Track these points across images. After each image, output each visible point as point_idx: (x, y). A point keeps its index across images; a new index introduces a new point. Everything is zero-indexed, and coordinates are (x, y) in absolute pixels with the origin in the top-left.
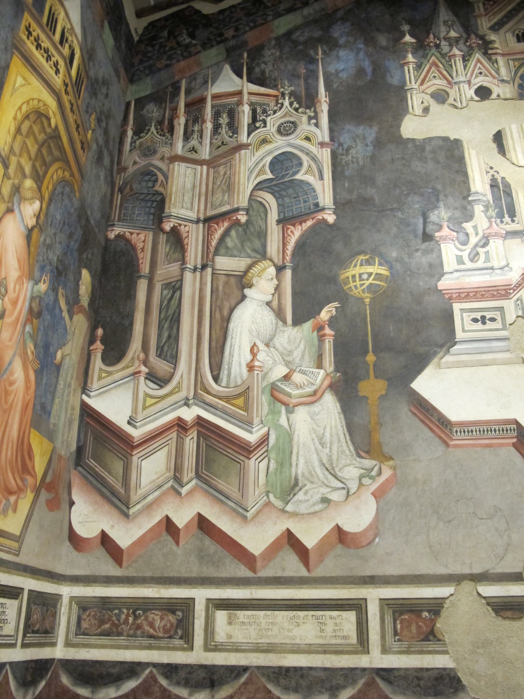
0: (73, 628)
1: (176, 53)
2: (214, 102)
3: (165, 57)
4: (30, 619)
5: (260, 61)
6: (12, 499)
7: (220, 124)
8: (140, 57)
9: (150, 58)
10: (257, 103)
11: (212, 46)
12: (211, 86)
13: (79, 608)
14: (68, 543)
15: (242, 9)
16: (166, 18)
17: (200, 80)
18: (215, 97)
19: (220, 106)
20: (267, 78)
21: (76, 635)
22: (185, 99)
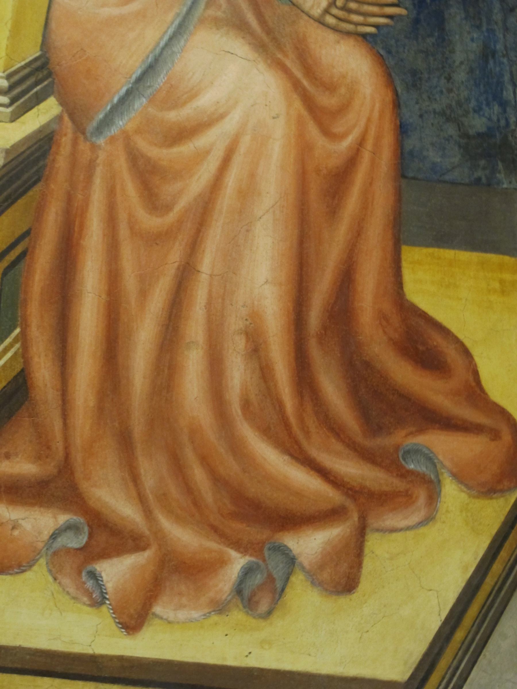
6: (309, 544)
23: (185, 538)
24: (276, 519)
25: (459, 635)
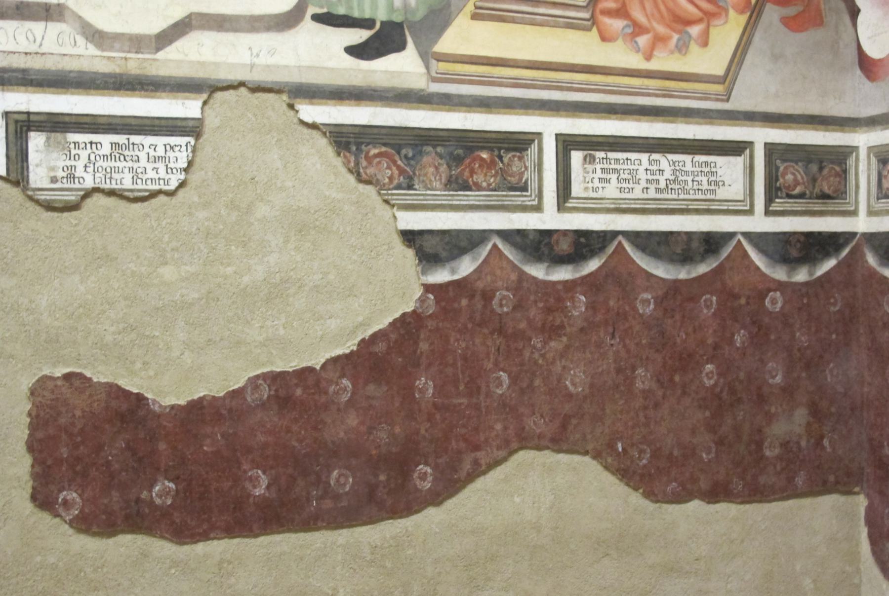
0: (874, 189)
4: (777, 180)
6: (695, 30)
13: (879, 161)
14: (858, 72)
21: (878, 199)
23: (661, 29)
24: (682, 22)
25: (736, 60)
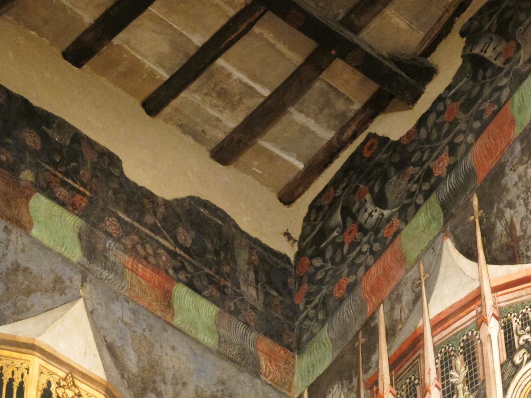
1: (360, 253)
2: (436, 338)
3: (345, 269)
5: (502, 205)
7: (453, 386)
8: (305, 287)
9: (322, 282)
10: (510, 306)
11: (418, 207)
12: (428, 303)
15: (454, 98)
16: (335, 183)
17: (407, 297)
18: (439, 324)
19: (447, 342)
20: (519, 239)
22: (388, 350)
